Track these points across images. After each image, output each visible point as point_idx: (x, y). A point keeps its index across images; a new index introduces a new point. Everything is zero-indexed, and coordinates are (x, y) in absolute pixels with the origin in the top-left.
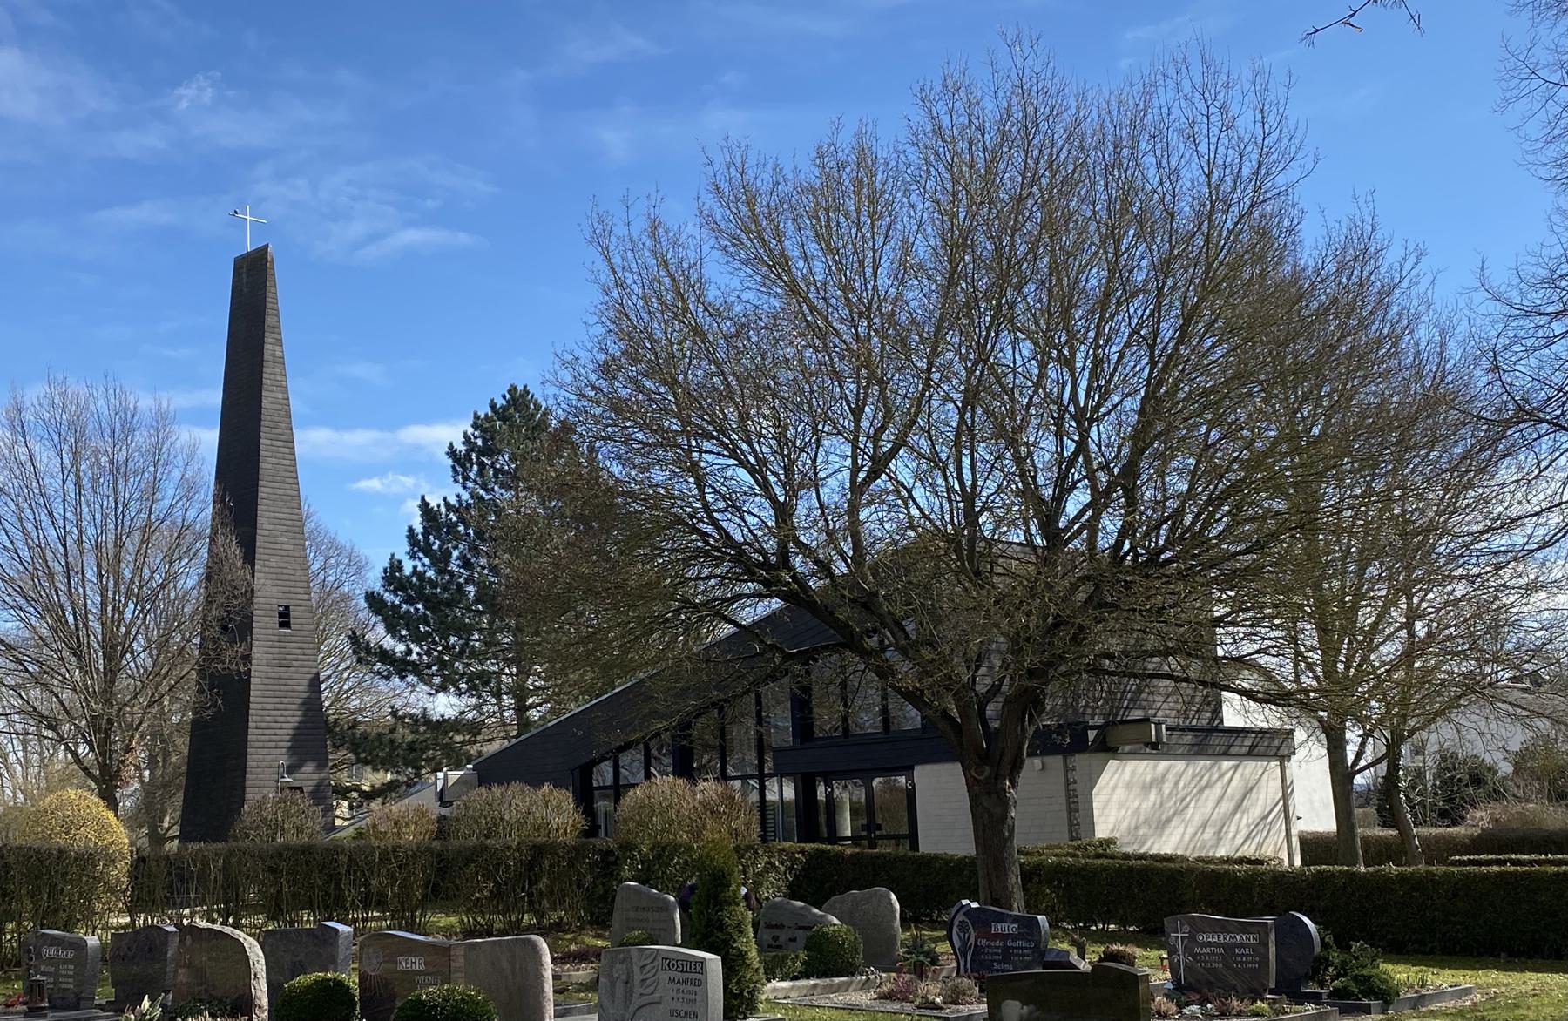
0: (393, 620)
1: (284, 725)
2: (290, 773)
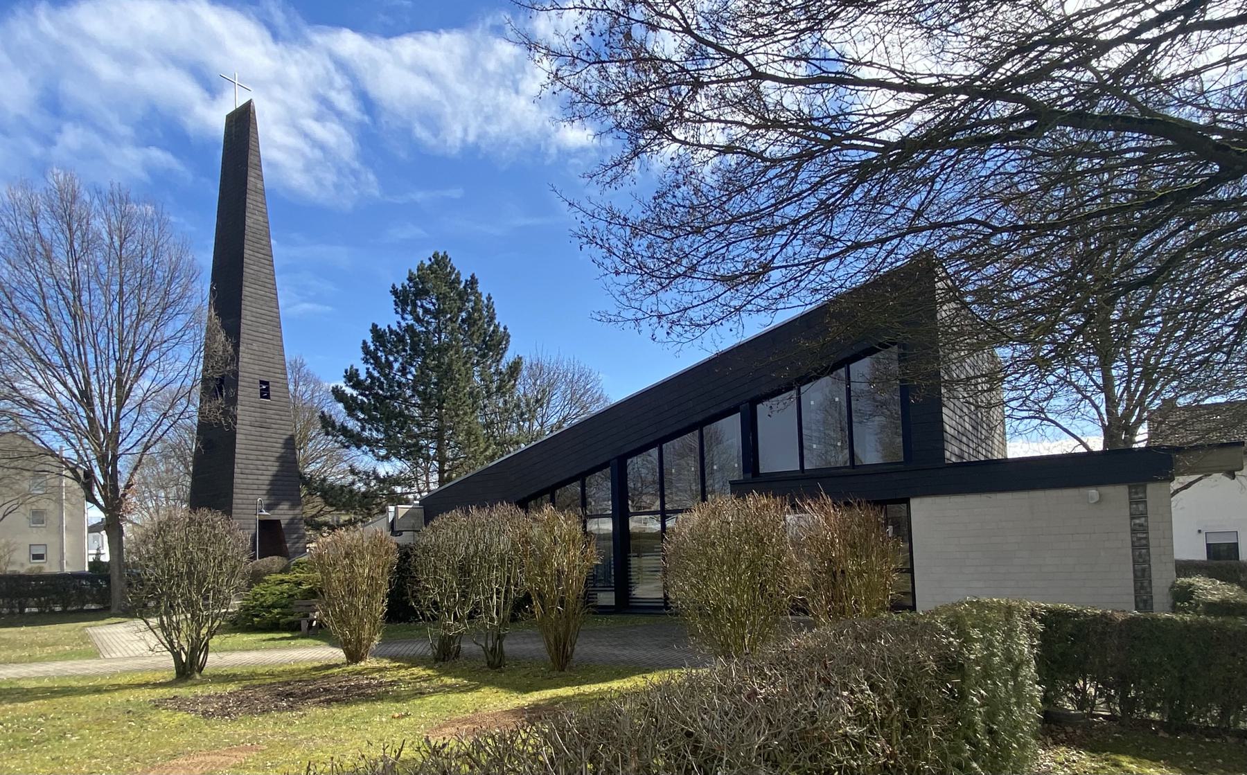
0: (351, 406)
1: (265, 472)
2: (268, 509)
